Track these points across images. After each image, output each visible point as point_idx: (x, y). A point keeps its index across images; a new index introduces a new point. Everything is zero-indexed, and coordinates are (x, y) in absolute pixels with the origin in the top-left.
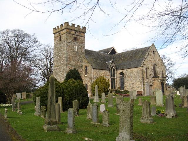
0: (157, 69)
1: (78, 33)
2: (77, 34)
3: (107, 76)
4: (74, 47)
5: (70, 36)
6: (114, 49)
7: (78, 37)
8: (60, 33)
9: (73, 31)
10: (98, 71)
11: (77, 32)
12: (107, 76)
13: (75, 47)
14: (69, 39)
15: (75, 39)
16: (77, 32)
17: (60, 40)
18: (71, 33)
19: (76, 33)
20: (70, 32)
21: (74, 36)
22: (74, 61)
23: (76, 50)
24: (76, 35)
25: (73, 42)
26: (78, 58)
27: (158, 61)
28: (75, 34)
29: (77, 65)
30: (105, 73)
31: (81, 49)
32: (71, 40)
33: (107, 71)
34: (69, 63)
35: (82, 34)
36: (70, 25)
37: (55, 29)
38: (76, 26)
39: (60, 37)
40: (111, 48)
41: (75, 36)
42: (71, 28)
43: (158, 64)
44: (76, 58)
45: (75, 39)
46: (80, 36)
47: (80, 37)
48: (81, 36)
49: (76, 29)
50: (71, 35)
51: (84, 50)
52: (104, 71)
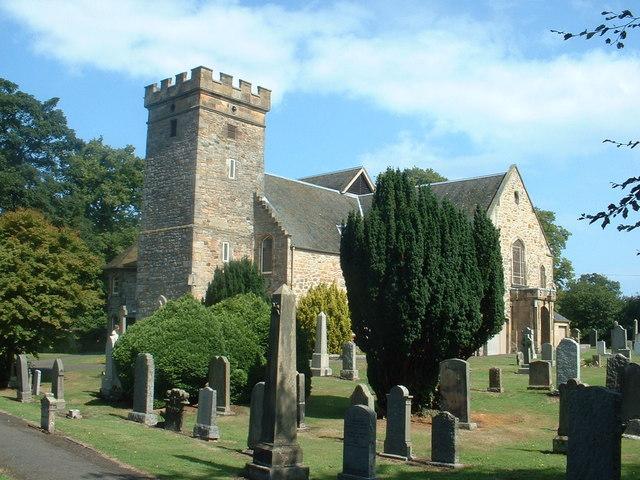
0: (527, 257)
2: (238, 113)
4: (223, 161)
6: (362, 175)
7: (240, 126)
8: (173, 107)
9: (225, 103)
13: (228, 162)
15: (232, 132)
17: (173, 134)
18: (218, 108)
19: (234, 109)
21: (226, 119)
22: (223, 214)
24: (232, 117)
26: (239, 204)
28: (230, 113)
29: (233, 232)
32: (214, 136)
37: (149, 88)
39: (174, 123)
40: (353, 172)
41: (232, 122)
42: (218, 92)
43: (527, 242)
45: (232, 132)
46: (248, 122)
47: (250, 126)
48: (252, 124)
49: (237, 95)
50: (215, 115)
51: (260, 176)
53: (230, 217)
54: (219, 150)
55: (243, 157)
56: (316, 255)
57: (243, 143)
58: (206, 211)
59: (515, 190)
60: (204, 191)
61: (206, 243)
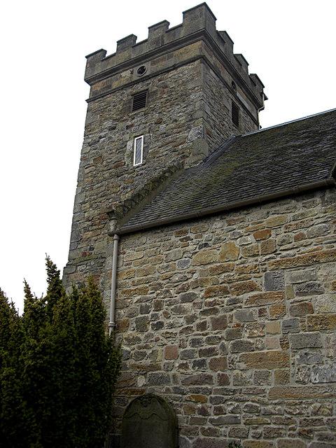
2: (149, 68)
3: (313, 260)
5: (109, 103)
7: (153, 85)
9: (126, 74)
10: (173, 238)
12: (313, 260)
18: (115, 85)
21: (129, 90)
25: (121, 125)
28: (136, 77)
30: (276, 237)
41: (140, 87)
46: (168, 71)
48: (175, 67)
52: (254, 216)
55: (159, 122)
56: (191, 231)
60: (87, 205)
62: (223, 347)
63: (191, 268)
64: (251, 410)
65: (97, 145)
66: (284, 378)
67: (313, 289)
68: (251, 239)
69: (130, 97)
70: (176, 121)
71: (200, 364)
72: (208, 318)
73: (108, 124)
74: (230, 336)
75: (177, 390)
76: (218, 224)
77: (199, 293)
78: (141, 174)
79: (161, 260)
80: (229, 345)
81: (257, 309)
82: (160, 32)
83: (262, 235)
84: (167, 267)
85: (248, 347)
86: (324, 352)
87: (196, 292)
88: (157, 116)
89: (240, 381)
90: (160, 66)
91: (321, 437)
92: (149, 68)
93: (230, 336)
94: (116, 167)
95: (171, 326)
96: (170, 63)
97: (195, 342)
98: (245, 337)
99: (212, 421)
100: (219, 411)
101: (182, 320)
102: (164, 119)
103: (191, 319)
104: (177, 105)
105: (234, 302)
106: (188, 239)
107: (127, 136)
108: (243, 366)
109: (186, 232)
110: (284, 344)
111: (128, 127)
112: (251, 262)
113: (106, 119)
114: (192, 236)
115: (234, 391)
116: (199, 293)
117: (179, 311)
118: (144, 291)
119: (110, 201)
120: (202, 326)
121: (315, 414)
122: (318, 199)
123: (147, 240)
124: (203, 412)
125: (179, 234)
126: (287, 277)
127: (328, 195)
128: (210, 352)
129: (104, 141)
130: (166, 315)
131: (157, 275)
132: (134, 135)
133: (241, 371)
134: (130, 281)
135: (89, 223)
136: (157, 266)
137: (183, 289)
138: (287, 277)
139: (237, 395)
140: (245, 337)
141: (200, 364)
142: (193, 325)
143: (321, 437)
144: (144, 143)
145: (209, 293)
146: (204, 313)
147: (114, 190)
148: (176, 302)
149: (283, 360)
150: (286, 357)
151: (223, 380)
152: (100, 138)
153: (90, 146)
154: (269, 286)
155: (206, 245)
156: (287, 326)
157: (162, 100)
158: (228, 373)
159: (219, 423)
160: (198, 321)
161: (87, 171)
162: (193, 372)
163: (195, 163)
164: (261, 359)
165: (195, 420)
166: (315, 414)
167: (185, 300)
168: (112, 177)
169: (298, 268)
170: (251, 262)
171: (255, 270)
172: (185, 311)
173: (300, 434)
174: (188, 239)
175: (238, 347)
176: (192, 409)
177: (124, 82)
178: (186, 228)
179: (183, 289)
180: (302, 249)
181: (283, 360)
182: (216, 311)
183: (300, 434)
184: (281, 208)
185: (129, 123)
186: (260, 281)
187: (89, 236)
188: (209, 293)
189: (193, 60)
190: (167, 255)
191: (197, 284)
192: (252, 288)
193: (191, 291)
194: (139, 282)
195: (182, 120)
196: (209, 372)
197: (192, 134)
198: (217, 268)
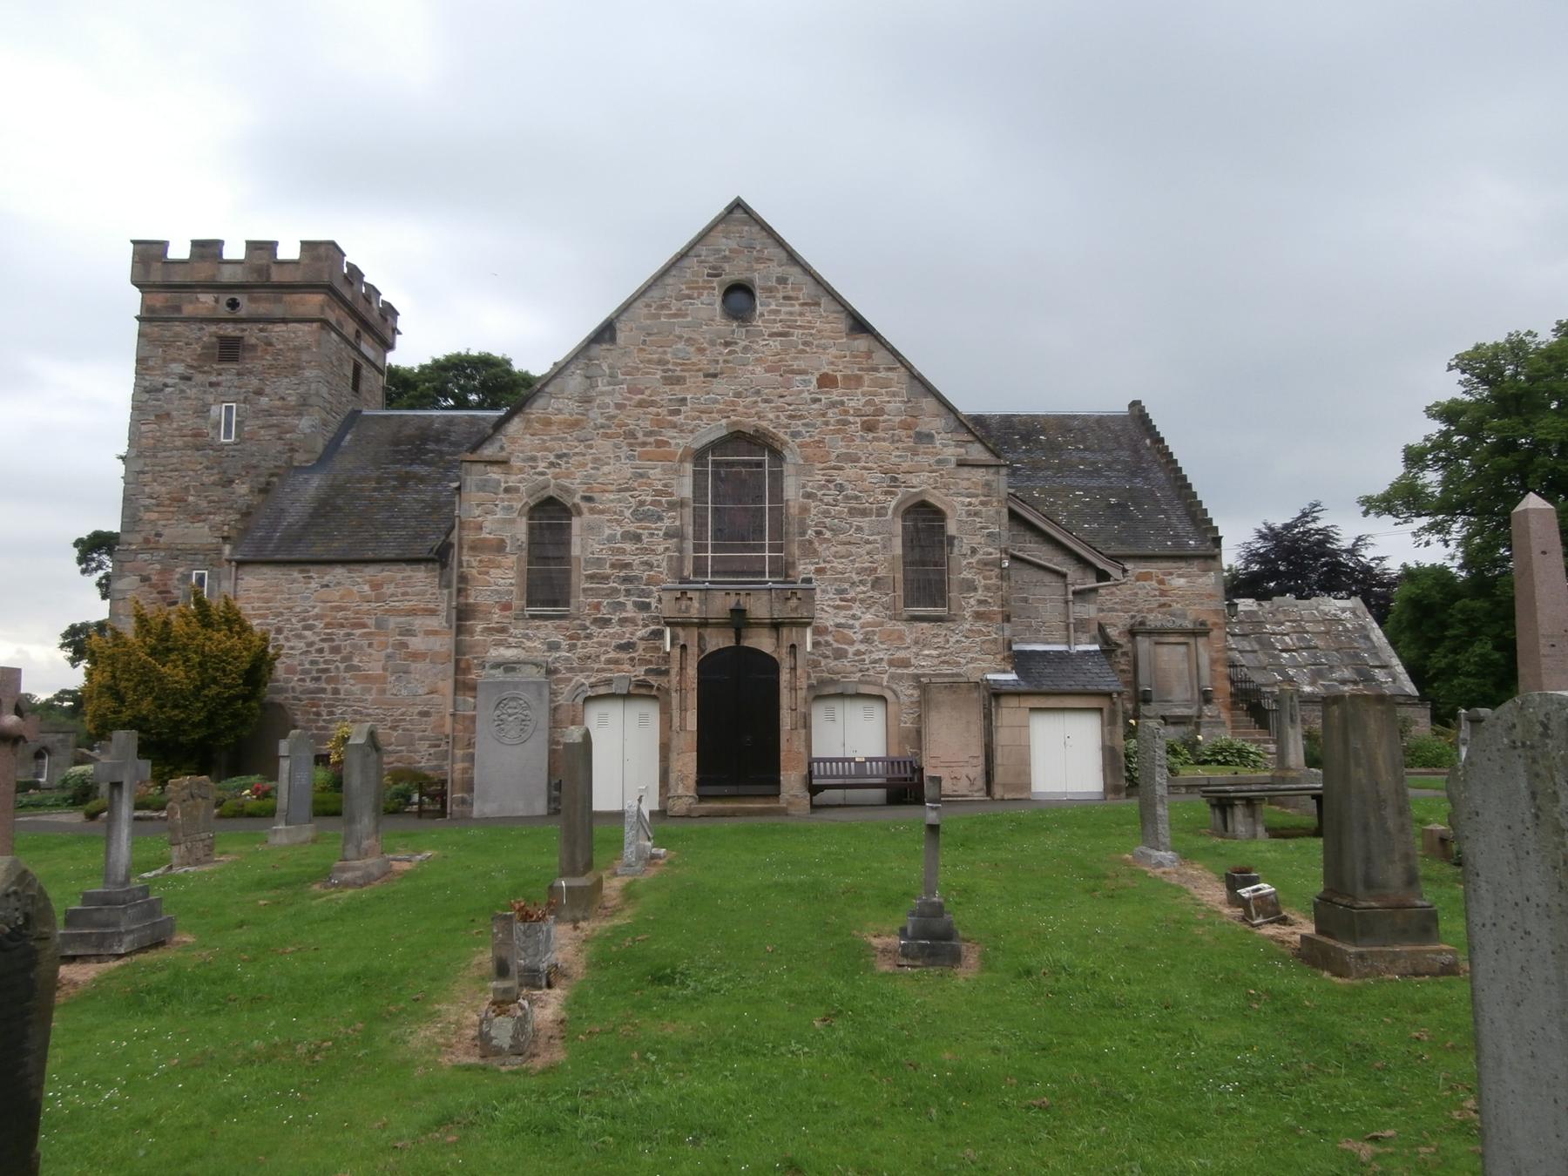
0: (792, 490)
1: (252, 300)
2: (246, 307)
3: (412, 612)
4: (203, 411)
5: (177, 335)
7: (252, 334)
9: (207, 299)
10: (296, 574)
11: (242, 298)
12: (412, 612)
13: (218, 411)
14: (166, 362)
16: (242, 298)
18: (188, 310)
19: (233, 304)
20: (178, 309)
21: (213, 328)
22: (197, 516)
23: (228, 434)
25: (199, 378)
27: (835, 395)
28: (224, 311)
30: (388, 589)
31: (274, 420)
33: (408, 571)
34: (147, 541)
35: (296, 297)
36: (179, 251)
38: (234, 251)
41: (230, 330)
44: (218, 493)
45: (230, 350)
47: (280, 328)
48: (284, 321)
49: (227, 275)
50: (179, 328)
52: (370, 571)
53: (218, 518)
54: (192, 392)
56: (314, 572)
57: (258, 365)
58: (147, 516)
59: (733, 273)
60: (148, 477)
61: (145, 579)
62: (337, 668)
63: (312, 604)
64: (356, 712)
65: (161, 396)
66: (383, 691)
67: (409, 632)
68: (366, 588)
69: (214, 339)
70: (283, 399)
71: (317, 679)
72: (325, 645)
73: (178, 368)
74: (344, 660)
75: (295, 698)
76: (339, 572)
77: (320, 625)
78: (233, 456)
79: (282, 592)
80: (342, 666)
81: (367, 642)
82: (261, 258)
83: (376, 586)
84: (289, 599)
85: (358, 668)
86: (412, 676)
87: (316, 623)
88: (255, 382)
89: (348, 692)
90: (263, 308)
91: (404, 730)
92: (246, 307)
93: (344, 660)
94: (195, 435)
95: (292, 648)
96: (278, 311)
97: (313, 663)
98: (356, 661)
99: (324, 720)
100: (331, 713)
101: (302, 644)
102: (267, 390)
103: (311, 644)
104: (286, 377)
105: (348, 635)
106: (311, 577)
107: (210, 398)
108: (352, 682)
109: (309, 571)
110: (385, 669)
111: (211, 384)
112: (365, 606)
113: (174, 360)
114: (315, 576)
115: (344, 700)
116: (320, 625)
117: (300, 637)
118: (264, 616)
119: (187, 479)
120: (321, 651)
121: (402, 715)
122: (423, 567)
123: (269, 572)
124: (318, 714)
125: (301, 571)
126: (393, 622)
127: (430, 566)
128: (326, 671)
129: (171, 393)
130: (287, 639)
131: (277, 605)
132: (223, 398)
133: (350, 686)
134: (249, 606)
135: (154, 501)
136: (279, 597)
137: (304, 620)
138: (393, 622)
139: (346, 703)
140: (356, 661)
141: (317, 679)
142: (312, 649)
143: (404, 730)
144: (237, 415)
145: (327, 626)
146: (323, 640)
147: (193, 467)
148: (296, 629)
149: (383, 679)
150: (385, 678)
151: (336, 691)
152: (166, 385)
153: (147, 392)
154: (379, 625)
155: (327, 586)
156: (389, 657)
157: (264, 362)
158: (339, 686)
159: (330, 721)
160: (317, 647)
161: (144, 428)
162: (309, 684)
163: (307, 461)
164: (367, 678)
165: (309, 721)
166: (402, 715)
167: (306, 628)
168: (186, 446)
169: (401, 616)
170: (365, 606)
171: (368, 613)
172: (304, 637)
173: (390, 728)
174: (311, 577)
175: (349, 668)
176: (309, 713)
177: (202, 312)
178: (308, 567)
179: (304, 620)
180: (406, 603)
181: (383, 679)
182: (333, 640)
183: (390, 728)
184: (395, 567)
185: (214, 379)
186: (371, 622)
187: (153, 518)
188: (327, 626)
189: (312, 321)
190: (289, 589)
191: (317, 617)
192: (364, 626)
193: (311, 622)
194: (259, 608)
195: (292, 400)
196: (324, 685)
197: (304, 423)
198: (336, 607)
